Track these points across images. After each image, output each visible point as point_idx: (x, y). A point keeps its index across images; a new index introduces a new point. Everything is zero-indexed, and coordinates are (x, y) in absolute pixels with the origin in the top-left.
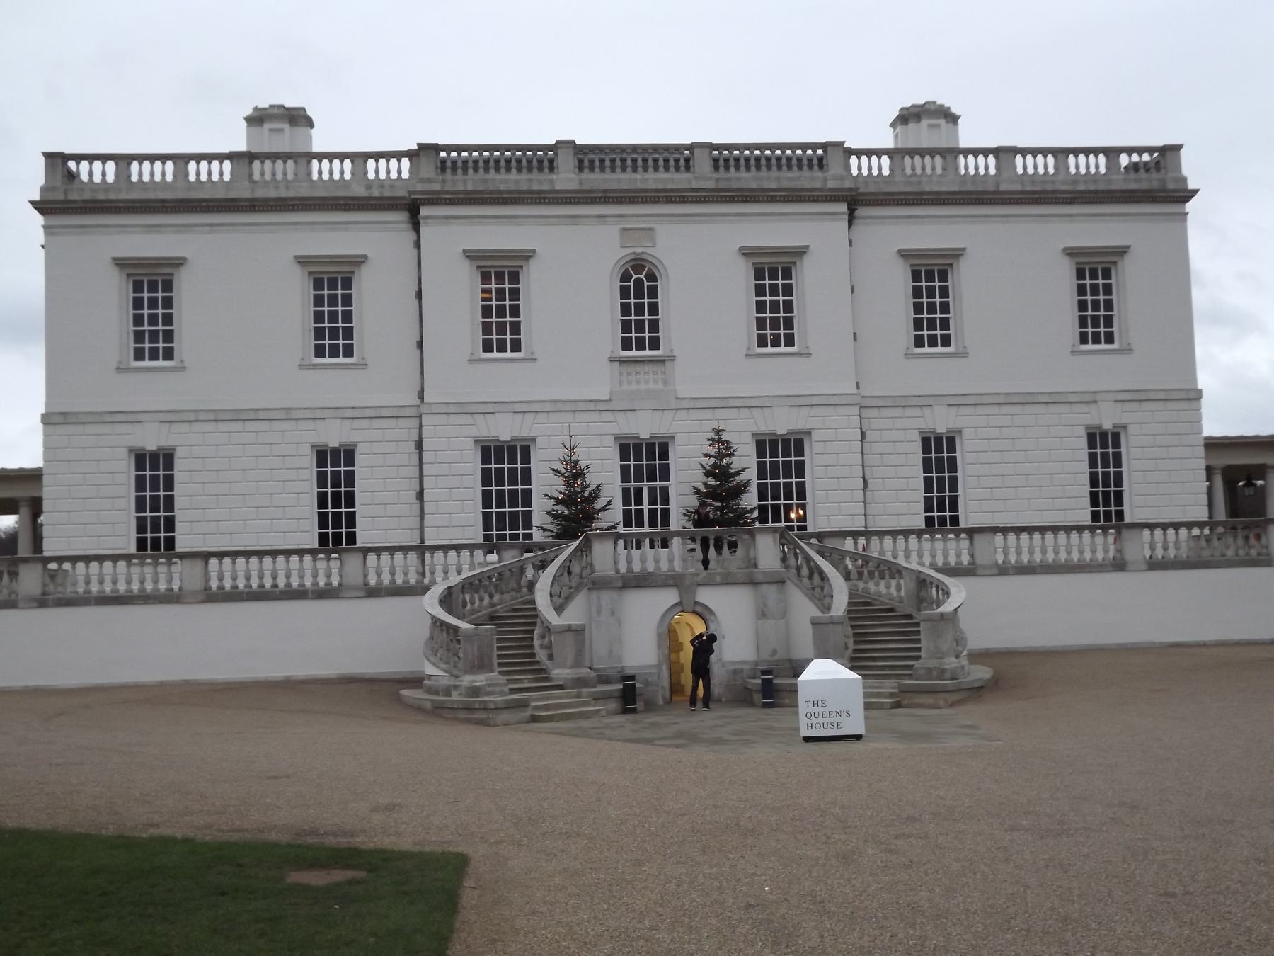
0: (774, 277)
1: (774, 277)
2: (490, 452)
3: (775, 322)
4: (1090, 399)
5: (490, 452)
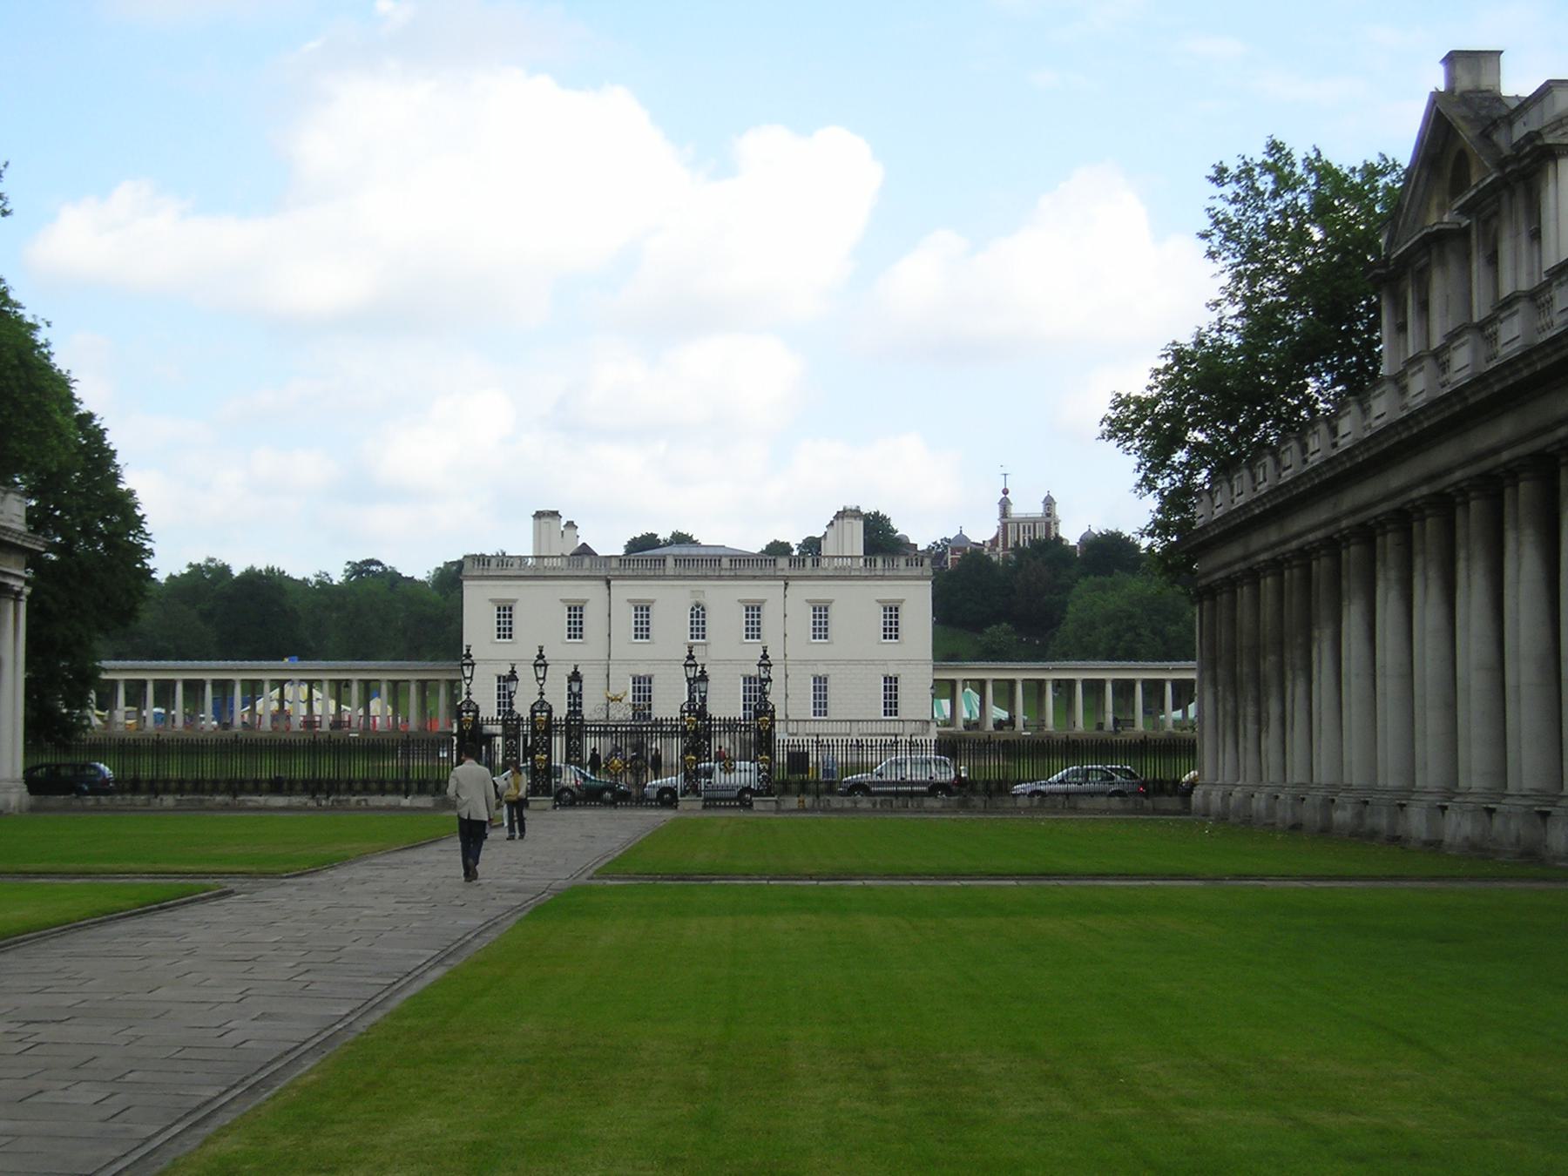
0: (754, 611)
1: (754, 611)
2: (637, 680)
3: (753, 629)
4: (885, 662)
5: (637, 680)
